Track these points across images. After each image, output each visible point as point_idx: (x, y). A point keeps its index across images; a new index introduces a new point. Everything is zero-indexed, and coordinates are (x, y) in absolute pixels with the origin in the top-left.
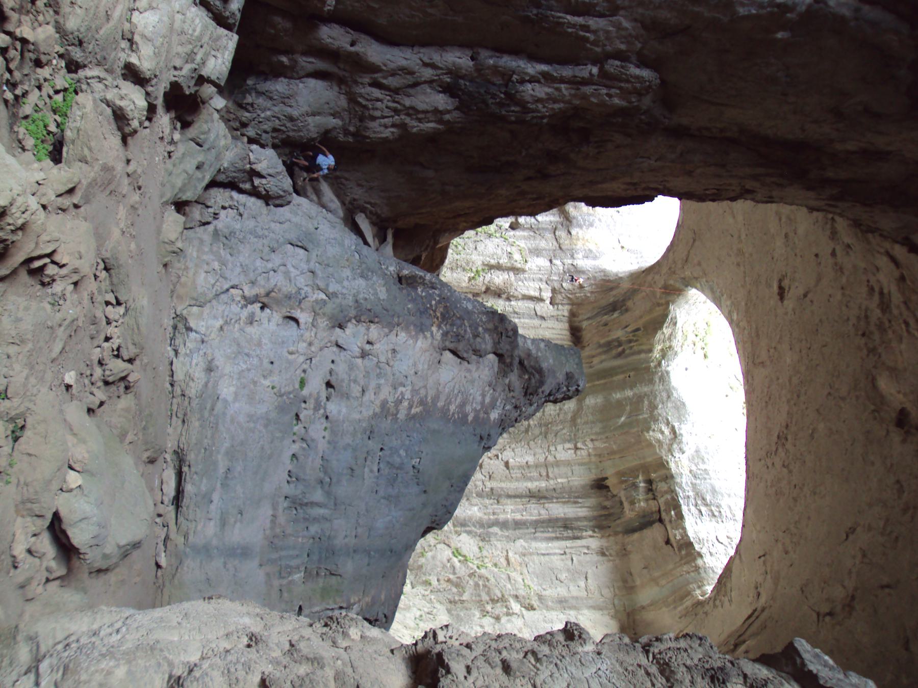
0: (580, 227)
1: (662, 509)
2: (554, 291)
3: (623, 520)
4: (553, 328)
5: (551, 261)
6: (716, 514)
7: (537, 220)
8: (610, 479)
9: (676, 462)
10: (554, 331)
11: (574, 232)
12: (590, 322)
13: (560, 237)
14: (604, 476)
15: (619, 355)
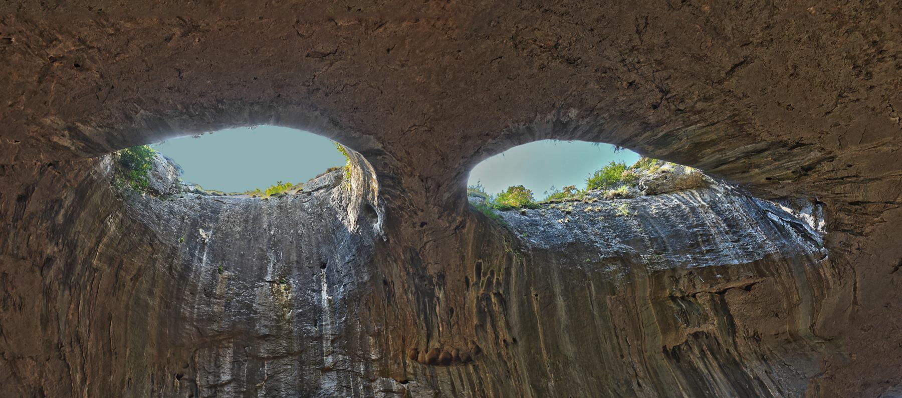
0: (251, 322)
1: (707, 289)
2: (385, 373)
3: (718, 335)
4: (452, 384)
5: (329, 370)
6: (705, 238)
7: (229, 382)
8: (667, 343)
9: (652, 264)
10: (457, 383)
11: (265, 331)
12: (436, 334)
13: (274, 351)
14: (662, 350)
15: (503, 302)
